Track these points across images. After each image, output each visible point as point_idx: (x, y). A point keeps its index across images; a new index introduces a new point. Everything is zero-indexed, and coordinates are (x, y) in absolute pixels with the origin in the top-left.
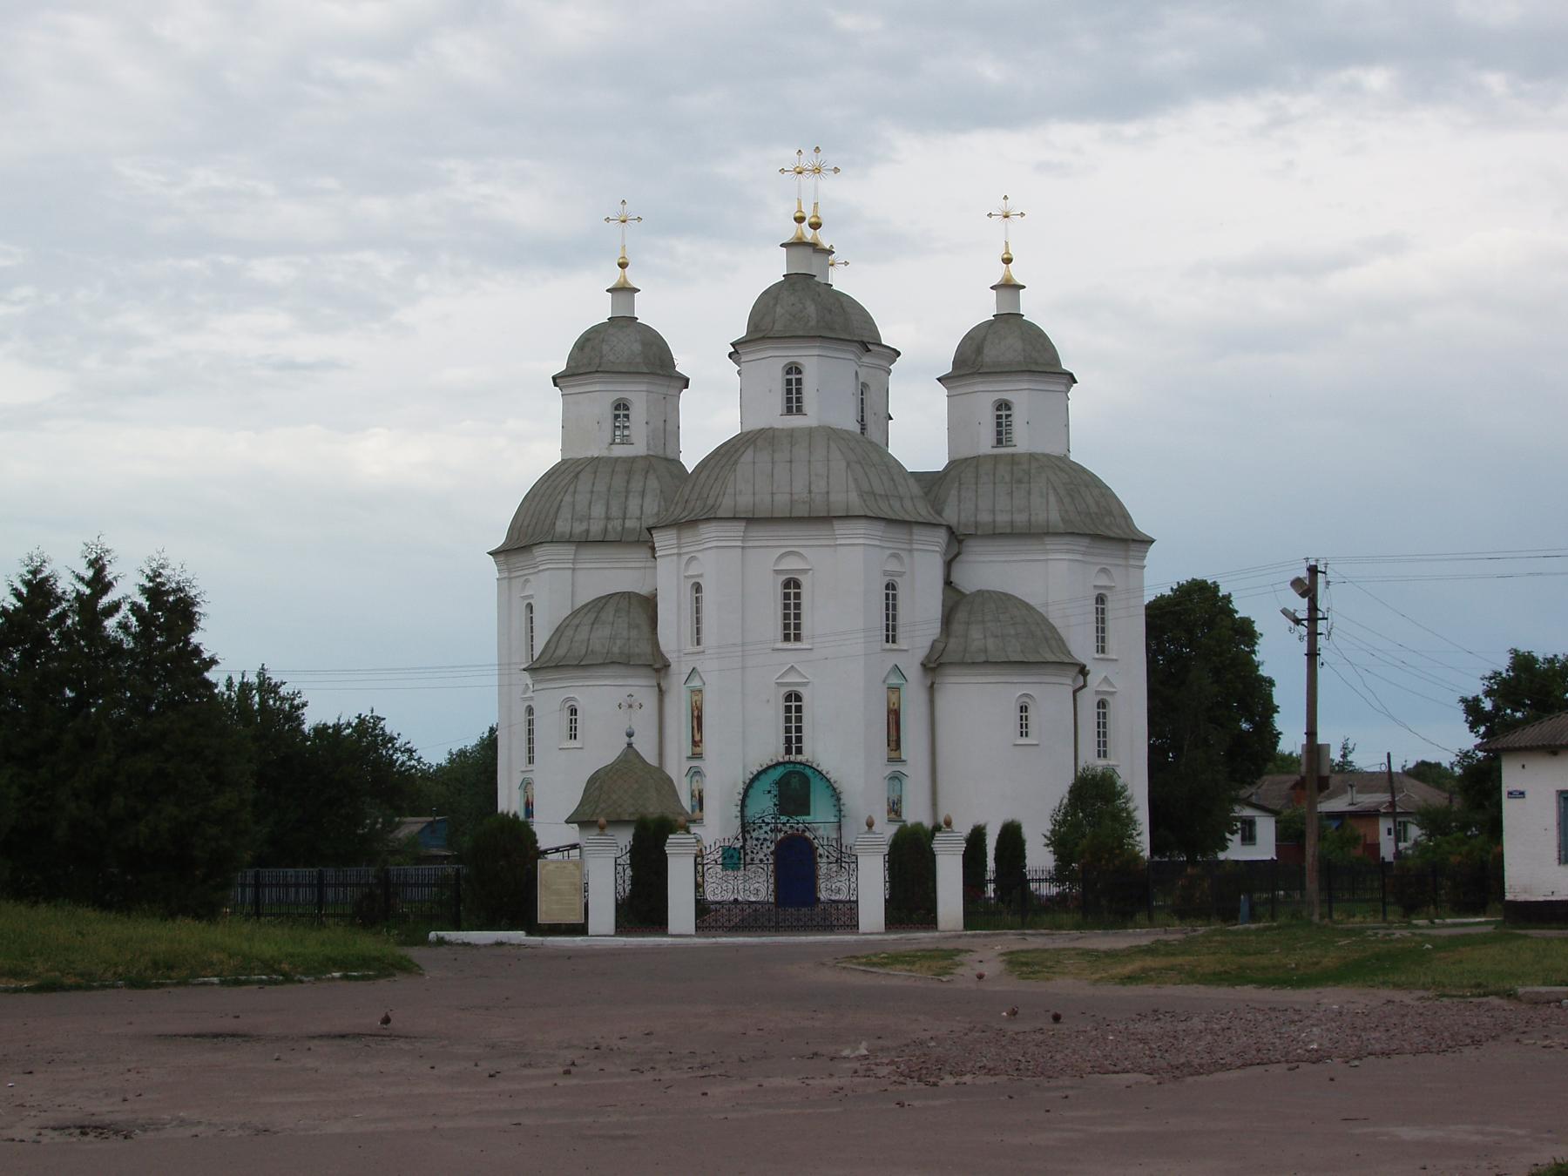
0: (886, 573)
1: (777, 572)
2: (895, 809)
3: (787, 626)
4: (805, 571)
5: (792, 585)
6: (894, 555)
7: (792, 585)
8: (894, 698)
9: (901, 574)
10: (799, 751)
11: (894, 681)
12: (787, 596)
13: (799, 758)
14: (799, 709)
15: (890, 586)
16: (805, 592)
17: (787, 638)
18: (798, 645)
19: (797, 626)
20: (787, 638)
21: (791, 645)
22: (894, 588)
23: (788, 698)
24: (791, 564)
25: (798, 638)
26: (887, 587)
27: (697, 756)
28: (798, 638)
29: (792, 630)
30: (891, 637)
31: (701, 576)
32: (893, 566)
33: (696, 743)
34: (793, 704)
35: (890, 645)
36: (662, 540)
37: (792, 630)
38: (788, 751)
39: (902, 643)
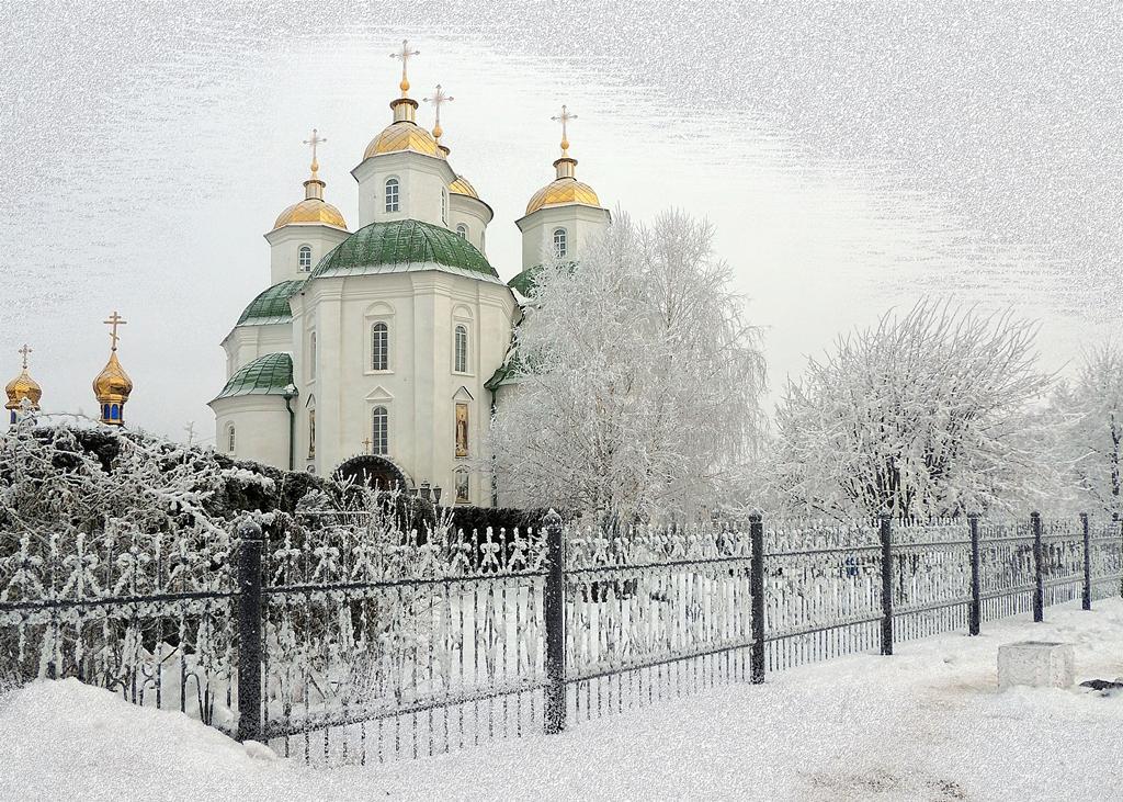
1: (368, 318)
2: (462, 493)
3: (376, 359)
4: (390, 316)
5: (381, 328)
6: (462, 306)
7: (381, 328)
8: (462, 411)
10: (385, 451)
11: (461, 398)
12: (376, 336)
13: (383, 456)
14: (384, 420)
17: (376, 367)
19: (385, 359)
20: (376, 367)
24: (381, 311)
25: (385, 367)
27: (311, 458)
28: (385, 367)
29: (380, 360)
30: (461, 365)
31: (314, 327)
32: (463, 313)
33: (312, 449)
34: (380, 416)
36: (296, 306)
37: (380, 360)
38: (376, 450)
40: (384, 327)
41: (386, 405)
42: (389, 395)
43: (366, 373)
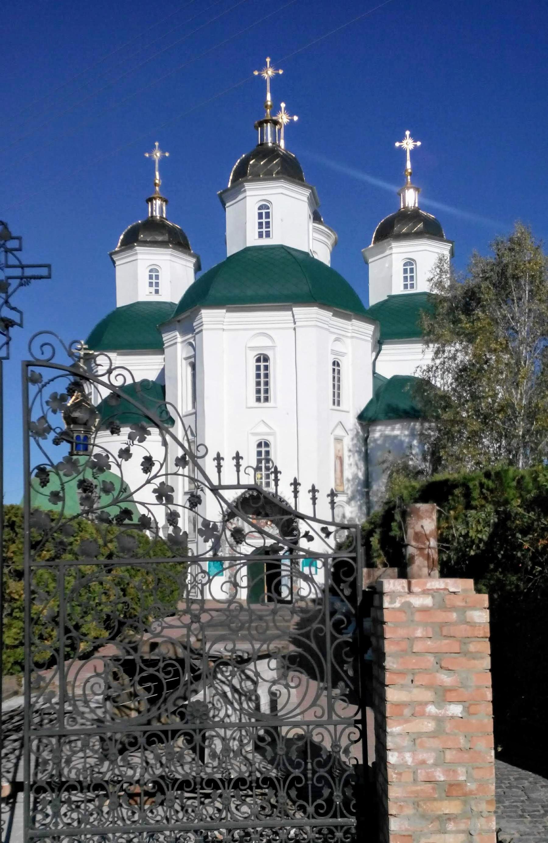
0: (333, 352)
3: (258, 391)
4: (273, 348)
5: (263, 359)
7: (263, 359)
8: (339, 446)
9: (343, 354)
11: (340, 432)
12: (258, 368)
15: (336, 364)
16: (271, 363)
17: (258, 400)
18: (266, 404)
21: (263, 404)
22: (338, 365)
23: (259, 445)
24: (262, 343)
25: (266, 399)
26: (334, 363)
28: (266, 399)
32: (339, 347)
35: (336, 407)
39: (343, 406)
40: (266, 359)
41: (270, 439)
42: (270, 428)
43: (249, 405)
